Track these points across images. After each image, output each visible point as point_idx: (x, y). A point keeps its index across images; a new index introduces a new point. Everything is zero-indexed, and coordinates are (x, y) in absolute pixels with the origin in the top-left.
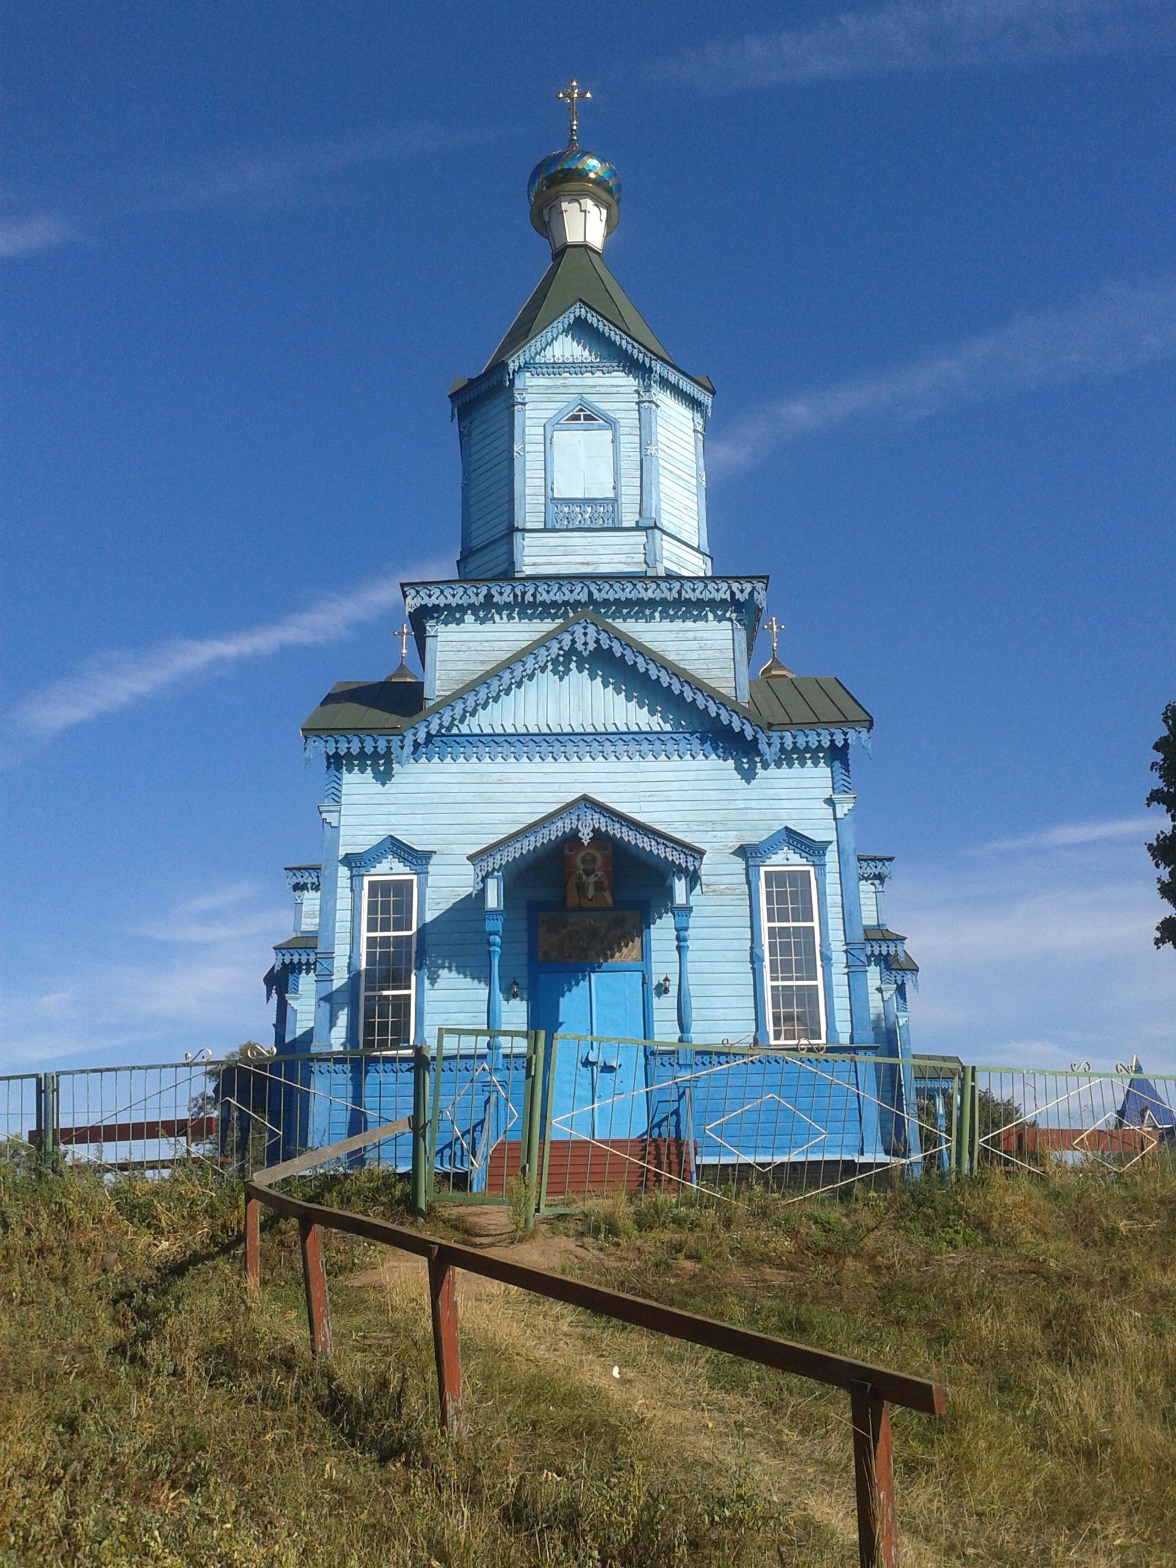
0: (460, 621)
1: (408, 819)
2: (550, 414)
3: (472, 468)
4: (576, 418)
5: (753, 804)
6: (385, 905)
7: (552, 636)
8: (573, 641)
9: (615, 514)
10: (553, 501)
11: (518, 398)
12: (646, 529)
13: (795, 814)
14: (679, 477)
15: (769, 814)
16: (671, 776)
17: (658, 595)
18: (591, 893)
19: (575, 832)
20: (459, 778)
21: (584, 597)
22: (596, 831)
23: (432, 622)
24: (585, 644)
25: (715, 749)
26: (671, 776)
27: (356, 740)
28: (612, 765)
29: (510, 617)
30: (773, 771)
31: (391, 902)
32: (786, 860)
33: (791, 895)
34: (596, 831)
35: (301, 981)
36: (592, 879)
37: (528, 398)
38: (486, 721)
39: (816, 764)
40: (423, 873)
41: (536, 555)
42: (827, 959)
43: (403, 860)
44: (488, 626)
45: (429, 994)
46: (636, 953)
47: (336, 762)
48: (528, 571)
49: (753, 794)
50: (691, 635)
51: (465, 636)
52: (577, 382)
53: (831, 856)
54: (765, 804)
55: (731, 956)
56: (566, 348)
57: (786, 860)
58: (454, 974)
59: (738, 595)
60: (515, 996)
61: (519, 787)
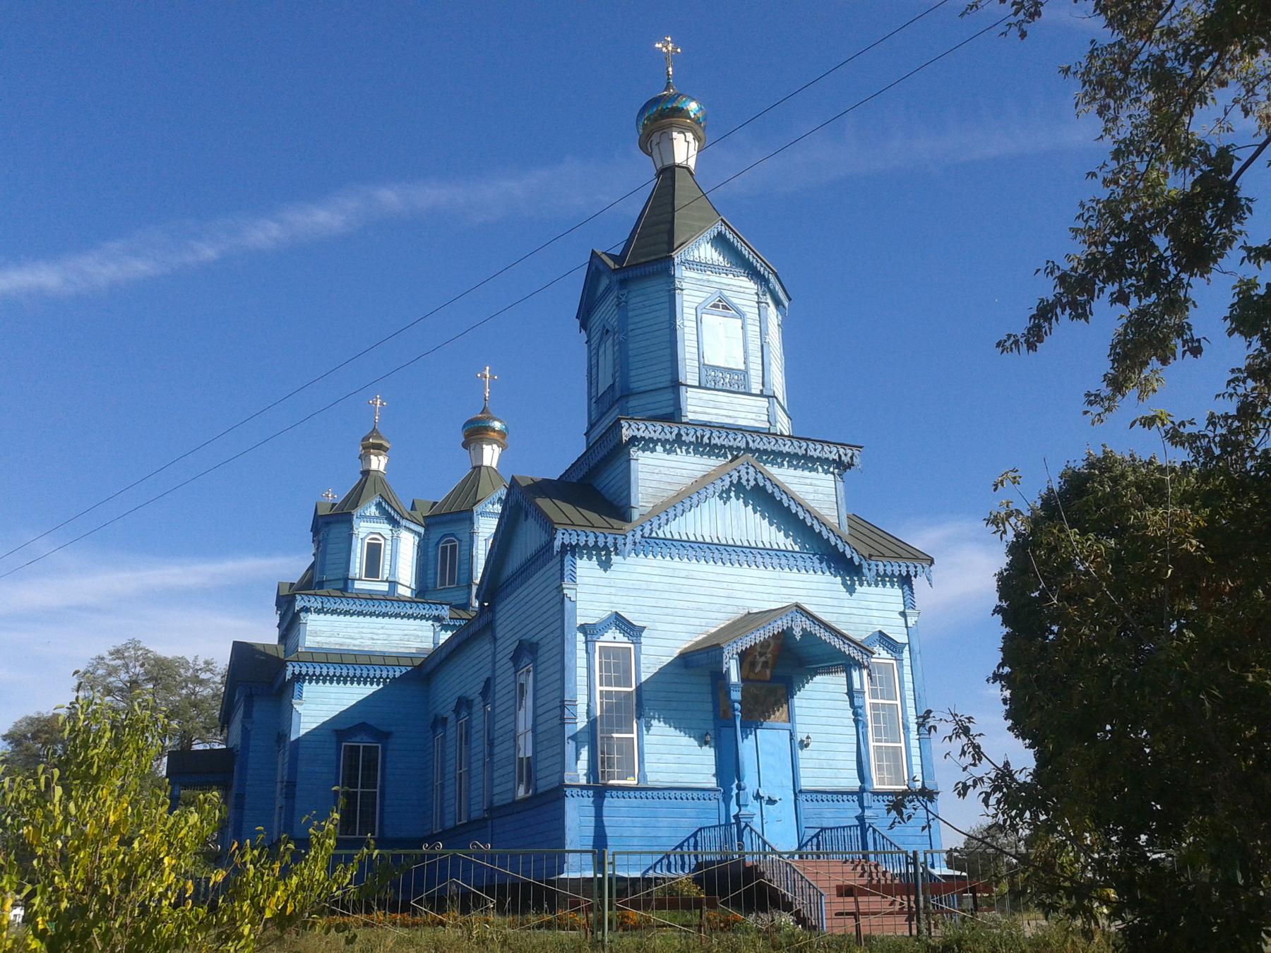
1: (624, 600)
2: (700, 300)
3: (630, 327)
4: (715, 306)
5: (855, 611)
6: (608, 664)
8: (740, 477)
10: (703, 366)
11: (678, 284)
12: (768, 397)
13: (882, 621)
15: (865, 620)
16: (801, 585)
17: (792, 450)
18: (758, 669)
20: (657, 571)
21: (743, 445)
23: (635, 449)
24: (748, 480)
25: (829, 568)
26: (801, 585)
27: (592, 535)
28: (762, 572)
29: (688, 452)
30: (865, 588)
31: (617, 664)
35: (304, 689)
36: (763, 659)
37: (685, 286)
38: (680, 527)
39: (892, 586)
40: (637, 643)
41: (699, 405)
43: (624, 633)
44: (672, 457)
45: (647, 738)
46: (784, 716)
48: (691, 416)
49: (854, 604)
50: (808, 481)
51: (657, 462)
52: (717, 279)
53: (906, 654)
54: (862, 612)
58: (662, 724)
59: (843, 458)
60: (706, 743)
61: (701, 583)
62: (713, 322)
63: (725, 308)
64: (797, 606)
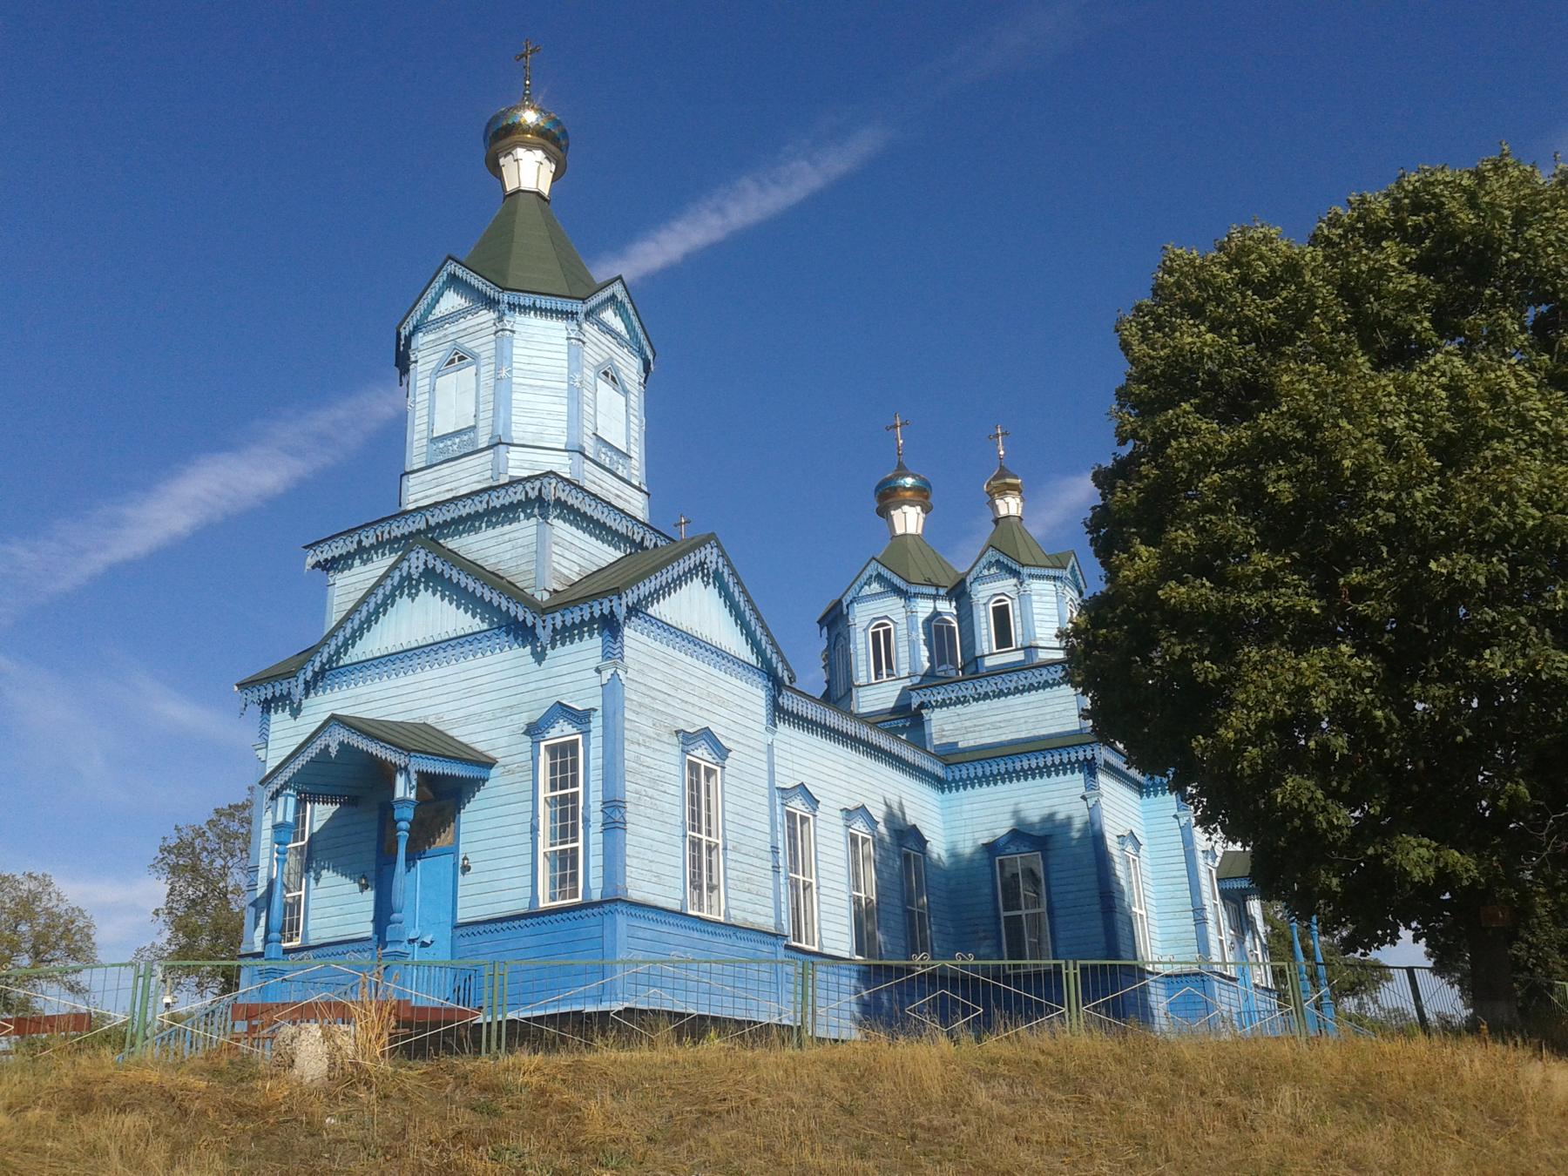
0: (351, 567)
2: (433, 365)
4: (452, 361)
5: (542, 684)
7: (393, 567)
9: (473, 442)
11: (413, 358)
14: (542, 387)
19: (327, 746)
22: (341, 744)
32: (562, 732)
34: (341, 744)
42: (586, 820)
47: (267, 706)
52: (454, 329)
53: (596, 723)
55: (516, 829)
56: (452, 301)
57: (562, 732)
62: (448, 382)
63: (461, 358)
64: (333, 718)
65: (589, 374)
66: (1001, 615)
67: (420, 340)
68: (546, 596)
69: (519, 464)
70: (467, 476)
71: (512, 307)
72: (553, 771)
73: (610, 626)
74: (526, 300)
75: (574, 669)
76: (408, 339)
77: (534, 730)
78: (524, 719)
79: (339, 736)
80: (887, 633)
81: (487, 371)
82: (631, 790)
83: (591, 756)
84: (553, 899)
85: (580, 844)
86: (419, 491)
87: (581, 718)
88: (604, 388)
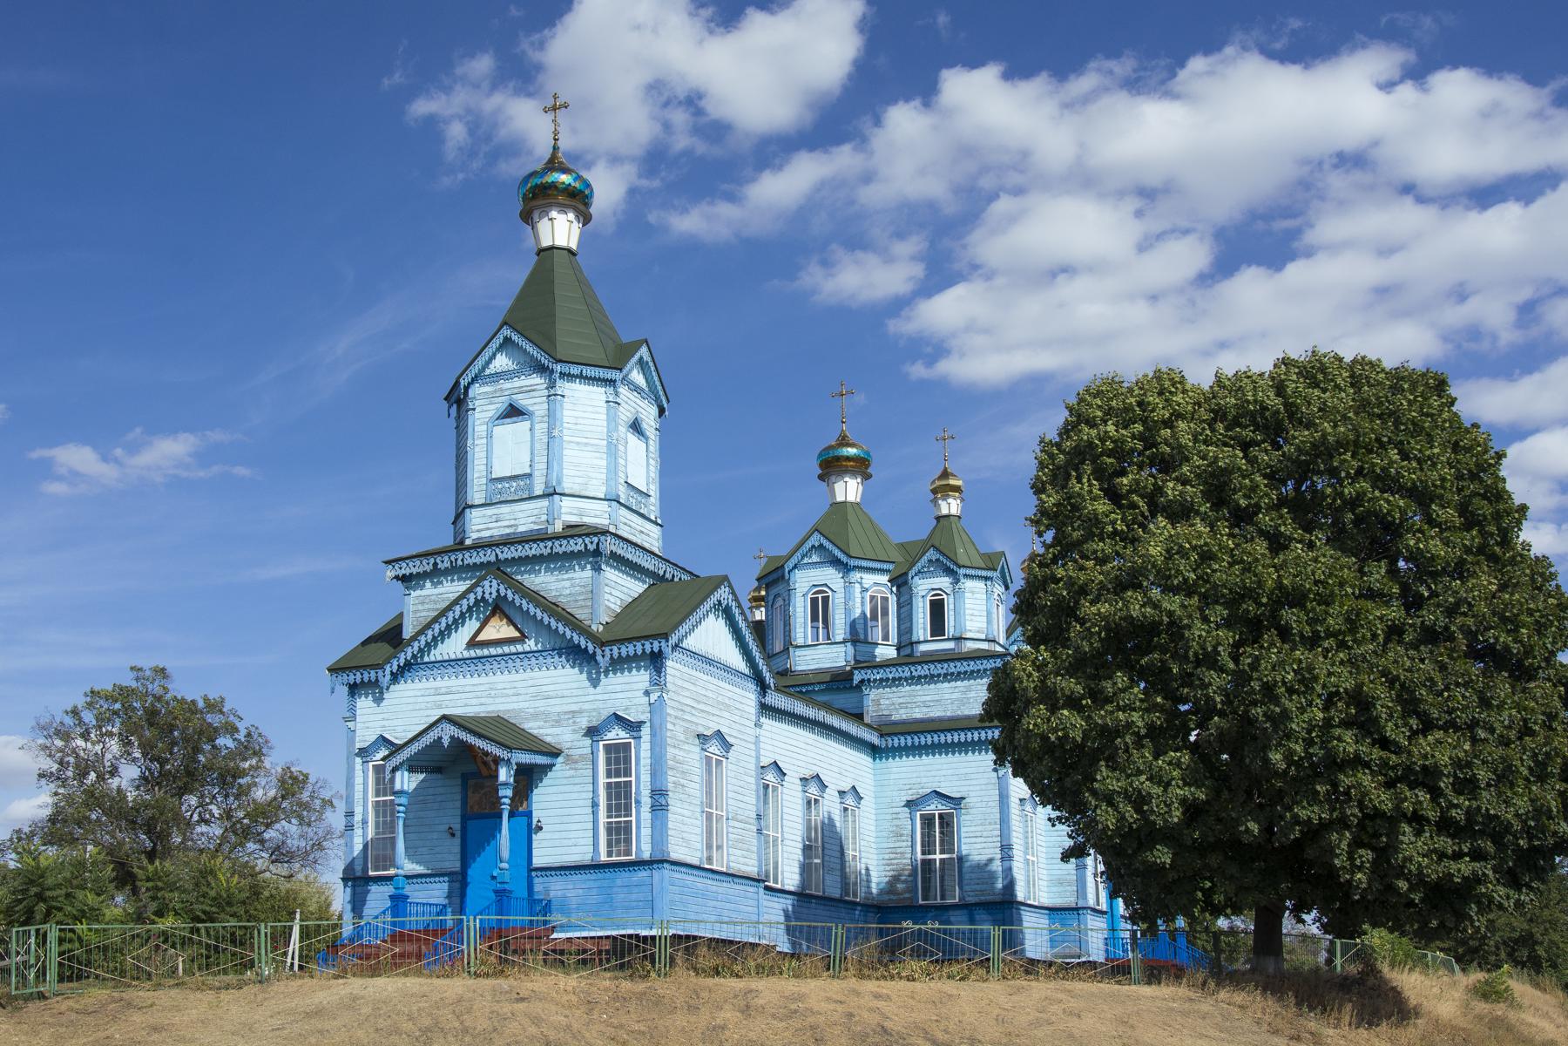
2: (490, 414)
7: (469, 591)
9: (530, 488)
32: (617, 735)
33: (619, 758)
42: (638, 802)
47: (354, 689)
53: (645, 731)
55: (581, 803)
57: (617, 735)
65: (623, 429)
66: (937, 608)
67: (476, 390)
68: (601, 628)
69: (569, 512)
70: (524, 517)
71: (563, 375)
72: (608, 762)
73: (656, 661)
74: (575, 370)
75: (626, 690)
76: (467, 388)
77: (593, 732)
78: (584, 723)
79: (447, 733)
80: (826, 600)
81: (541, 428)
82: (671, 780)
83: (642, 754)
84: (610, 854)
85: (633, 818)
86: (480, 525)
87: (633, 727)
88: (633, 439)
